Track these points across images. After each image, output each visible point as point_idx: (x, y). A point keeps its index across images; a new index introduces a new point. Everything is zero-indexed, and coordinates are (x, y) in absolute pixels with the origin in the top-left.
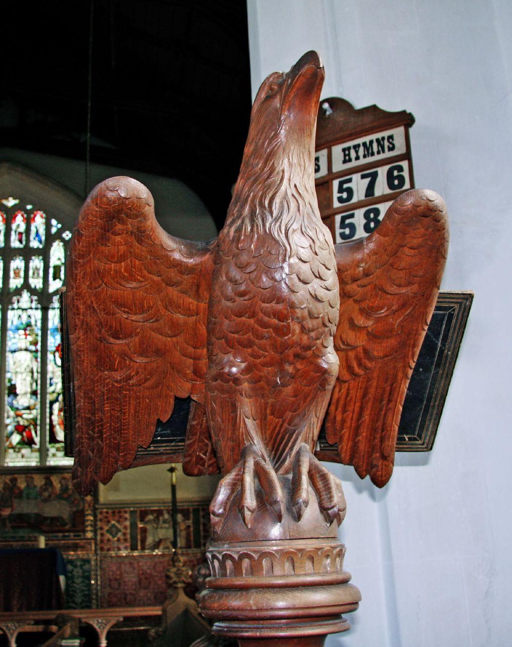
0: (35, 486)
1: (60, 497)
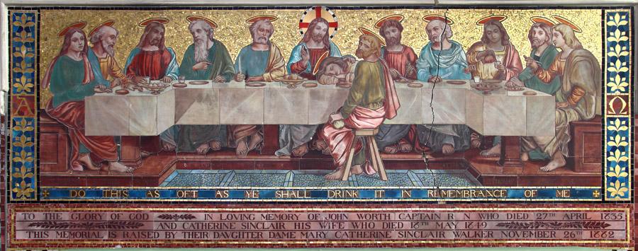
0: (454, 45)
1: (531, 79)
